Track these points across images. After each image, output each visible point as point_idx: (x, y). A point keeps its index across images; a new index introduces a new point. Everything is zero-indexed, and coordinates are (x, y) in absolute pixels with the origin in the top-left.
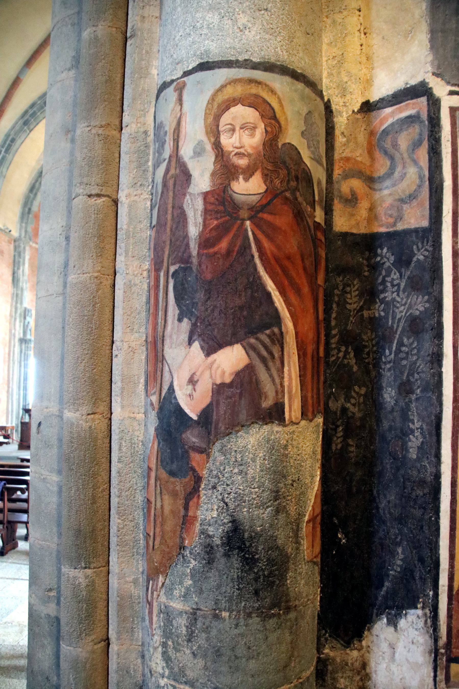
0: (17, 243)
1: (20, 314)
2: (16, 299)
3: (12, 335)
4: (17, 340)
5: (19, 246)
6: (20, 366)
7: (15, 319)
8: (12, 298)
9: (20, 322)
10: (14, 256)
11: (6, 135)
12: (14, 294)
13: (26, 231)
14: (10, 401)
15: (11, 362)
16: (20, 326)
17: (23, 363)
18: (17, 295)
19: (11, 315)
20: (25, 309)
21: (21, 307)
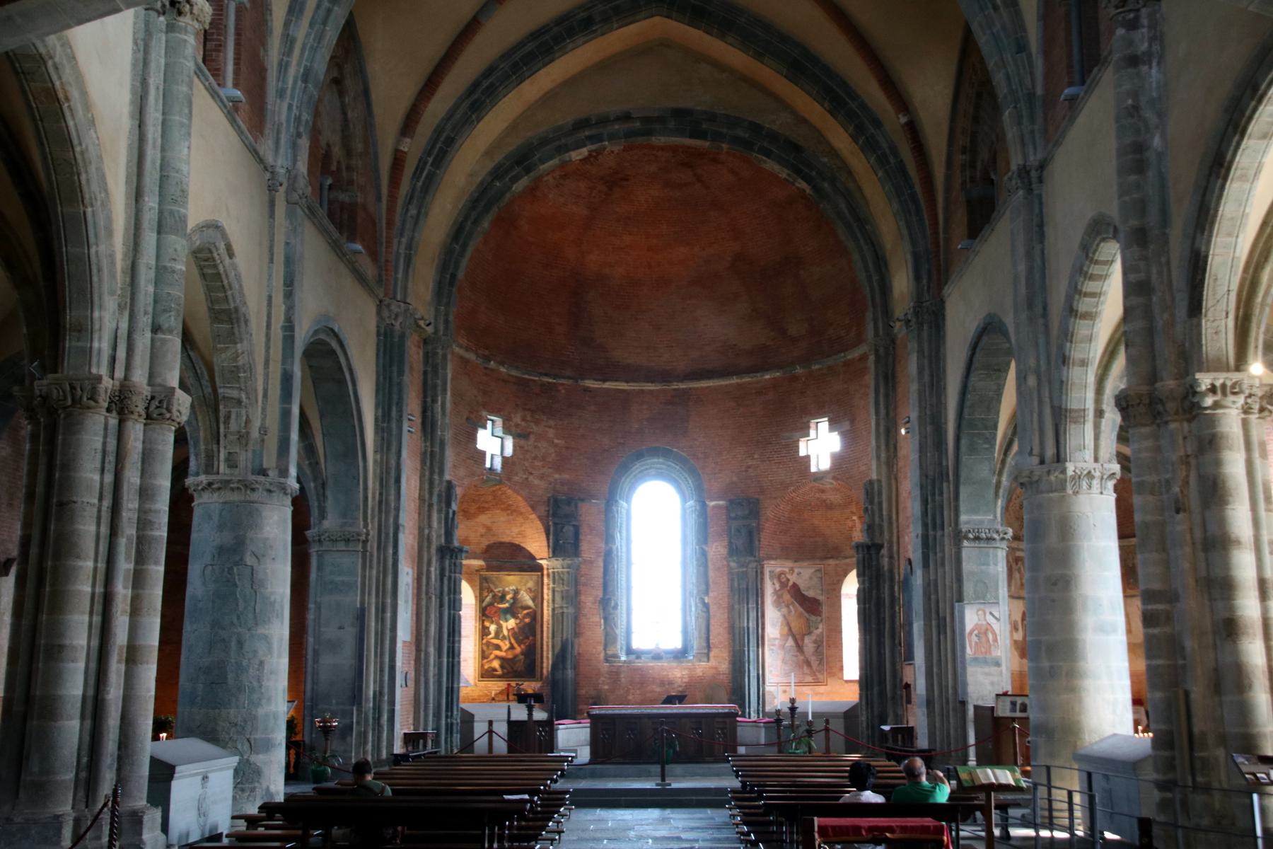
0: (430, 347)
1: (439, 496)
2: (431, 463)
3: (423, 539)
4: (433, 550)
5: (435, 354)
6: (441, 605)
7: (430, 506)
8: (423, 462)
9: (439, 511)
10: (425, 373)
11: (435, 131)
12: (425, 452)
13: (447, 322)
14: (422, 679)
15: (424, 596)
16: (439, 522)
17: (446, 599)
18: (432, 454)
19: (421, 499)
20: (449, 482)
21: (441, 481)
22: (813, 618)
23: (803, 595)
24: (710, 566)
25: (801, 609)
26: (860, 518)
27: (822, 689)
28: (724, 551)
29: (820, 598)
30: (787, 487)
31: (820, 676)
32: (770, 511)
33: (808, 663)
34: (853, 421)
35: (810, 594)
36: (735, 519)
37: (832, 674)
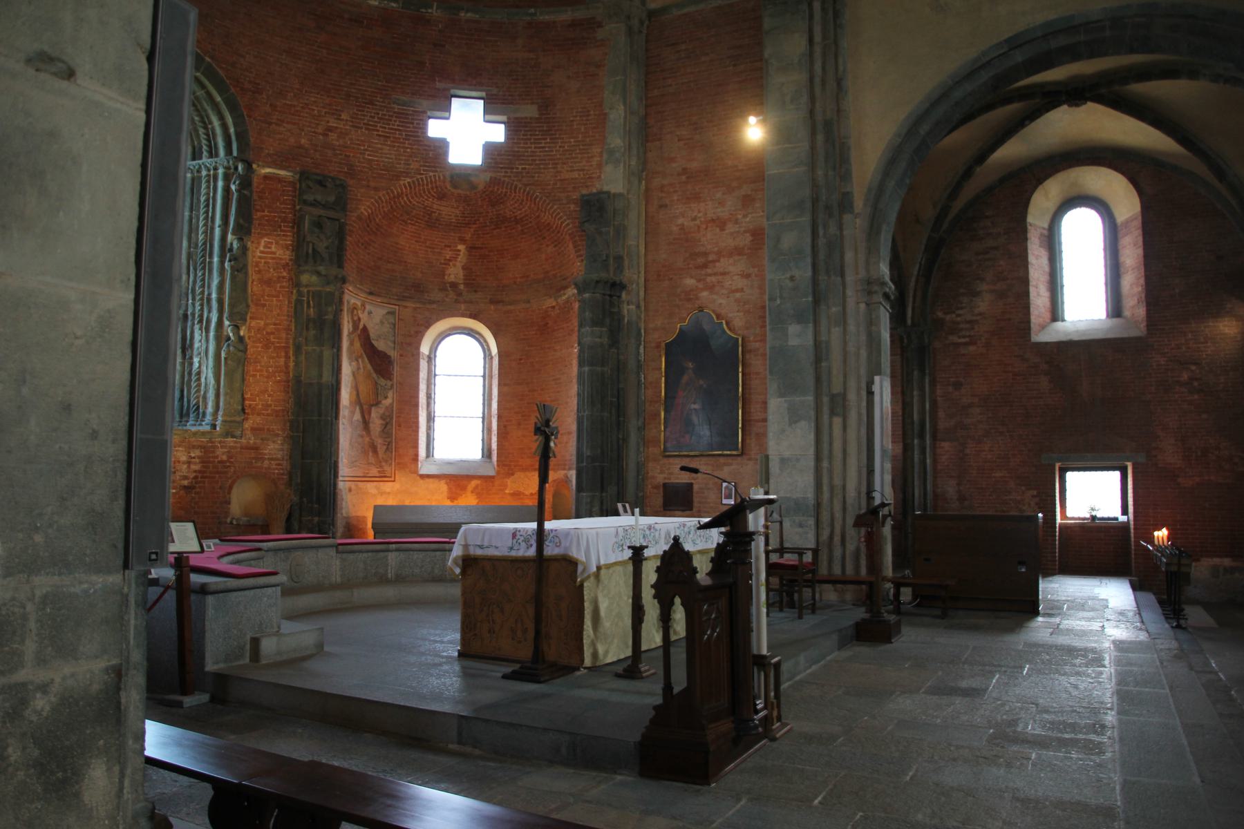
22: (382, 382)
23: (373, 346)
24: (252, 275)
25: (369, 366)
26: (471, 249)
27: (387, 487)
28: (286, 255)
29: (393, 354)
30: (397, 177)
31: (386, 468)
32: (364, 205)
33: (375, 450)
34: (546, 106)
35: (381, 345)
36: (315, 204)
37: (401, 466)
